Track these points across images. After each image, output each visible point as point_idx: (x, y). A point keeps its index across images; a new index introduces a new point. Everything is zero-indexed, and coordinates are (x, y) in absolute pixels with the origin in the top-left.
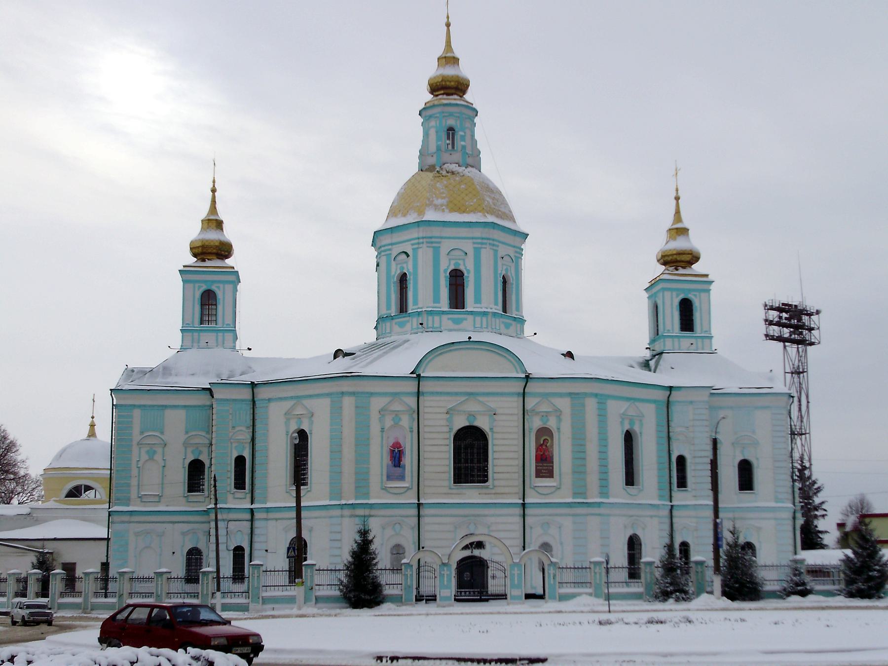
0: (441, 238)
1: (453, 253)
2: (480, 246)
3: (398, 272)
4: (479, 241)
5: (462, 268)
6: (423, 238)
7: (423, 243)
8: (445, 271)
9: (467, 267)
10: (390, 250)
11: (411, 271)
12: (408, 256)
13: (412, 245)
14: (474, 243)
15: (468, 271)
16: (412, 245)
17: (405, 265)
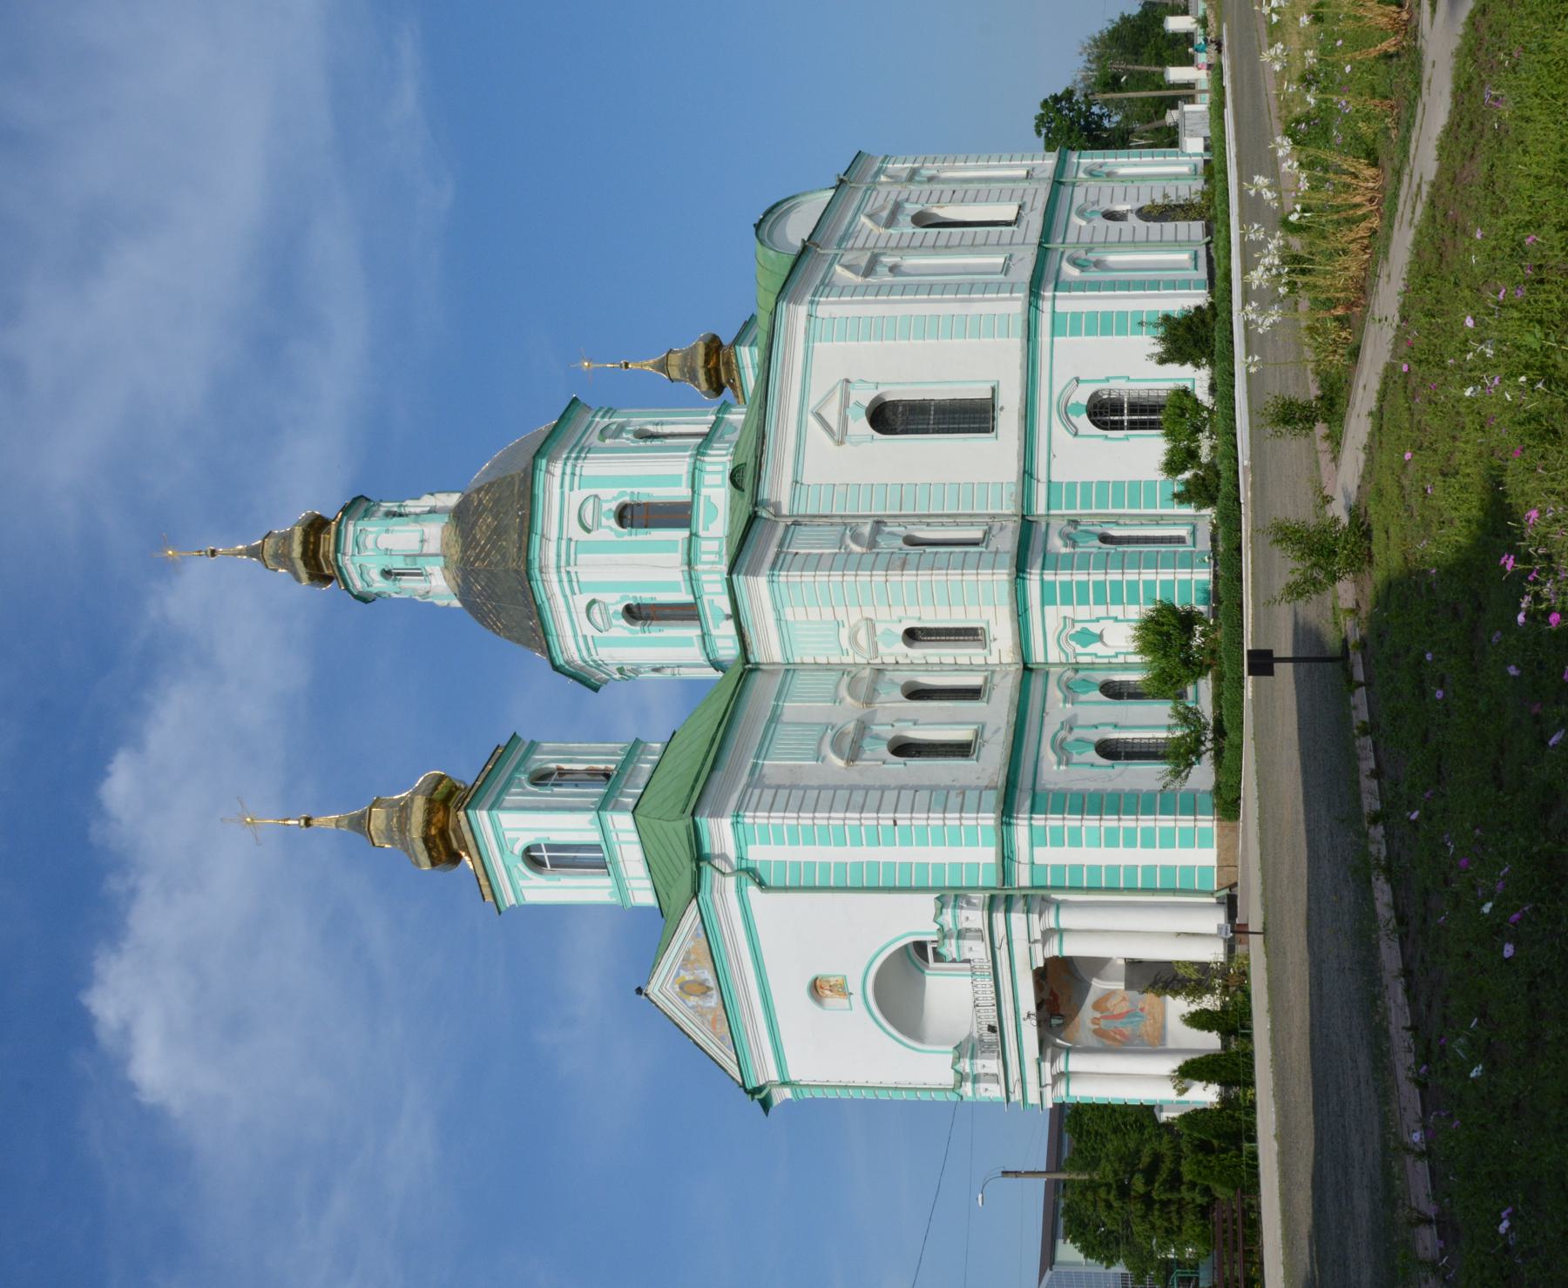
0: (560, 539)
1: (588, 520)
2: (577, 478)
3: (623, 622)
4: (567, 478)
5: (614, 506)
6: (559, 572)
7: (568, 573)
8: (618, 535)
9: (612, 498)
10: (585, 637)
11: (618, 596)
12: (593, 602)
13: (573, 593)
14: (571, 489)
15: (623, 494)
16: (573, 593)
17: (611, 609)
